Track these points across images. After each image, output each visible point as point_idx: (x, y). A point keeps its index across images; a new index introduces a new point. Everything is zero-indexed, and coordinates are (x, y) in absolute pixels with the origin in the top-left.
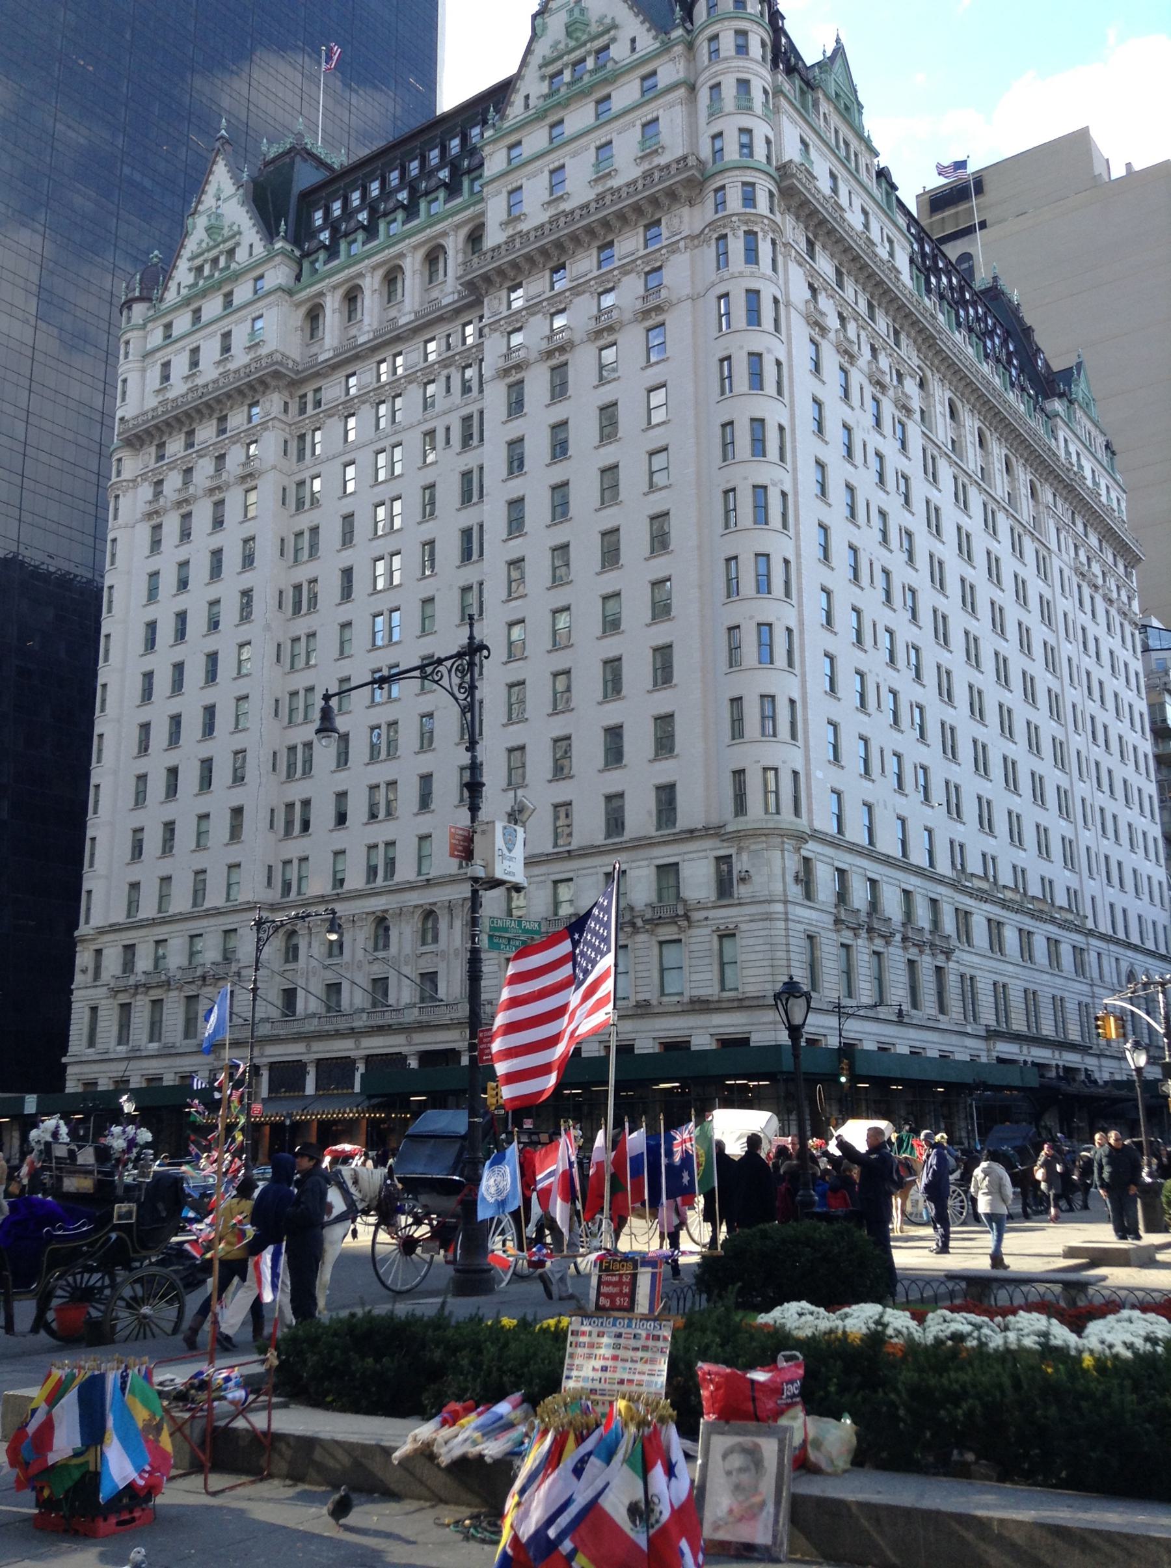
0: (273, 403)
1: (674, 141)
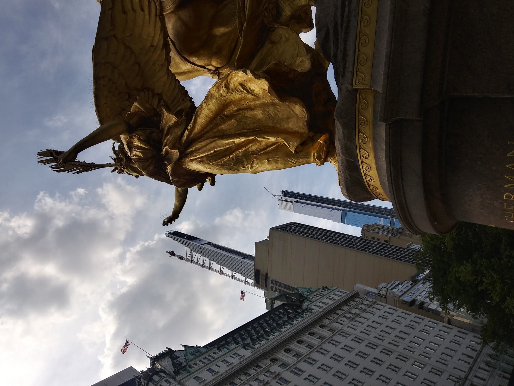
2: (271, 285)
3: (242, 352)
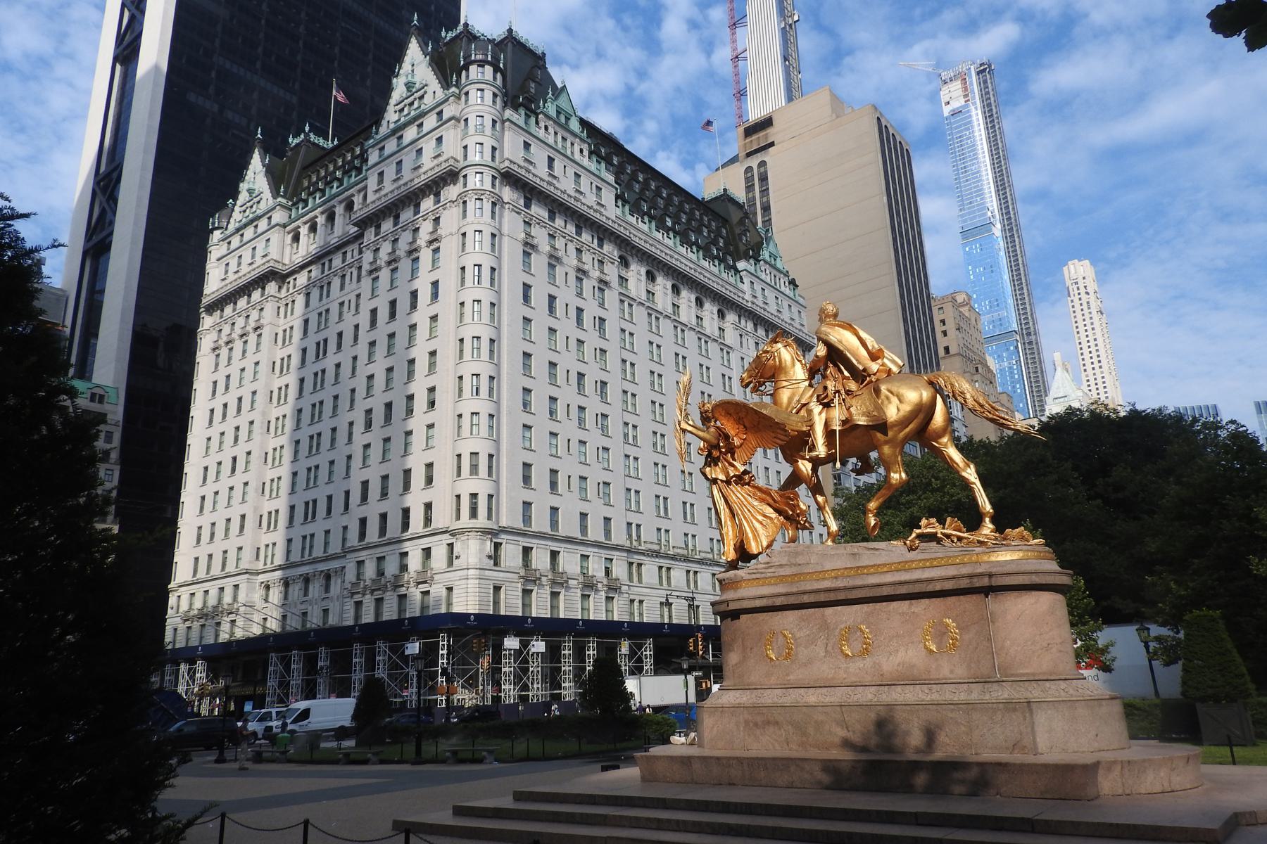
0: (272, 287)
1: (451, 148)
2: (754, 162)
3: (608, 196)
